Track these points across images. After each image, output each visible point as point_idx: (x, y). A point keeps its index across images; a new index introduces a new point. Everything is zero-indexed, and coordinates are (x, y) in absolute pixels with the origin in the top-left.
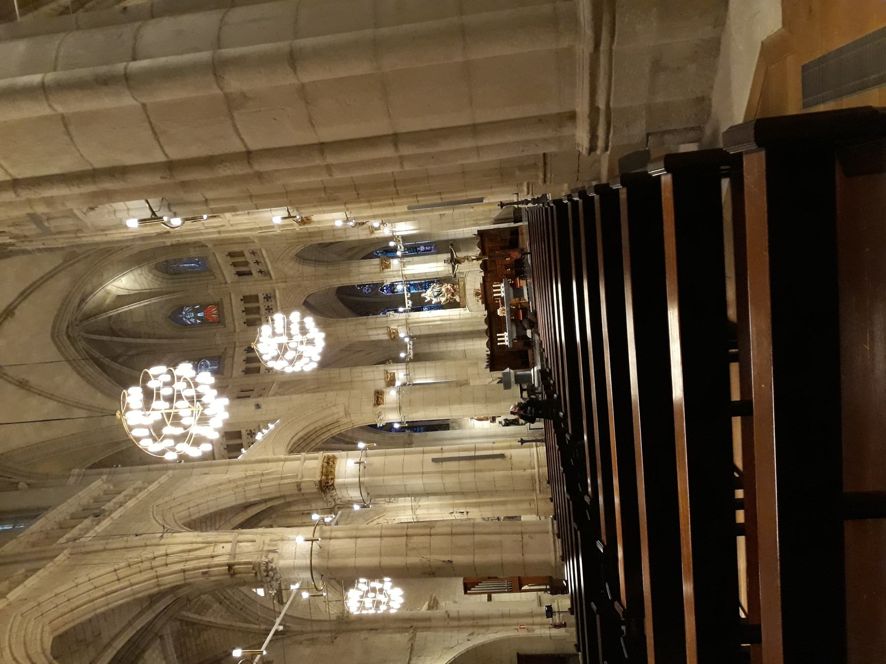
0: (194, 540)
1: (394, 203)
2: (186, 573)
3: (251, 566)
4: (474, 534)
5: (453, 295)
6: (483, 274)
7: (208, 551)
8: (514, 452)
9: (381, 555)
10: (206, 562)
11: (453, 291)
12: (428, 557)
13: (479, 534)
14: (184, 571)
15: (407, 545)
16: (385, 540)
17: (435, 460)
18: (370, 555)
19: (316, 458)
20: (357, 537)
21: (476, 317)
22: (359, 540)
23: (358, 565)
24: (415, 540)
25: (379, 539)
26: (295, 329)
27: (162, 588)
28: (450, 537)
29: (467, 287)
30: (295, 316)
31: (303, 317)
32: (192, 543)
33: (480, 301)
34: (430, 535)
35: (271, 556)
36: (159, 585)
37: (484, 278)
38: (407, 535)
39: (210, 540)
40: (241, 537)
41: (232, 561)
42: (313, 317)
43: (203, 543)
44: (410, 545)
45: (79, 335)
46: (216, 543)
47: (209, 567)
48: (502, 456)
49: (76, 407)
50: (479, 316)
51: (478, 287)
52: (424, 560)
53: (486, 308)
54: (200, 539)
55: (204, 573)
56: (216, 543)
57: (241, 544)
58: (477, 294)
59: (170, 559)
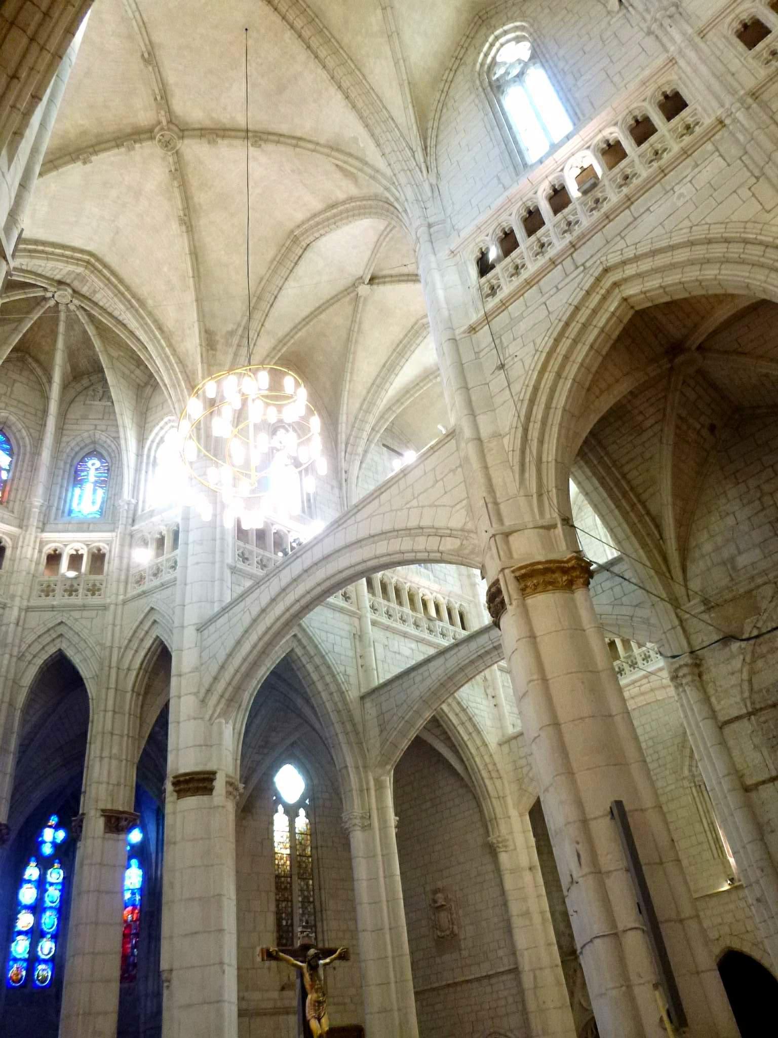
45: (53, 296)
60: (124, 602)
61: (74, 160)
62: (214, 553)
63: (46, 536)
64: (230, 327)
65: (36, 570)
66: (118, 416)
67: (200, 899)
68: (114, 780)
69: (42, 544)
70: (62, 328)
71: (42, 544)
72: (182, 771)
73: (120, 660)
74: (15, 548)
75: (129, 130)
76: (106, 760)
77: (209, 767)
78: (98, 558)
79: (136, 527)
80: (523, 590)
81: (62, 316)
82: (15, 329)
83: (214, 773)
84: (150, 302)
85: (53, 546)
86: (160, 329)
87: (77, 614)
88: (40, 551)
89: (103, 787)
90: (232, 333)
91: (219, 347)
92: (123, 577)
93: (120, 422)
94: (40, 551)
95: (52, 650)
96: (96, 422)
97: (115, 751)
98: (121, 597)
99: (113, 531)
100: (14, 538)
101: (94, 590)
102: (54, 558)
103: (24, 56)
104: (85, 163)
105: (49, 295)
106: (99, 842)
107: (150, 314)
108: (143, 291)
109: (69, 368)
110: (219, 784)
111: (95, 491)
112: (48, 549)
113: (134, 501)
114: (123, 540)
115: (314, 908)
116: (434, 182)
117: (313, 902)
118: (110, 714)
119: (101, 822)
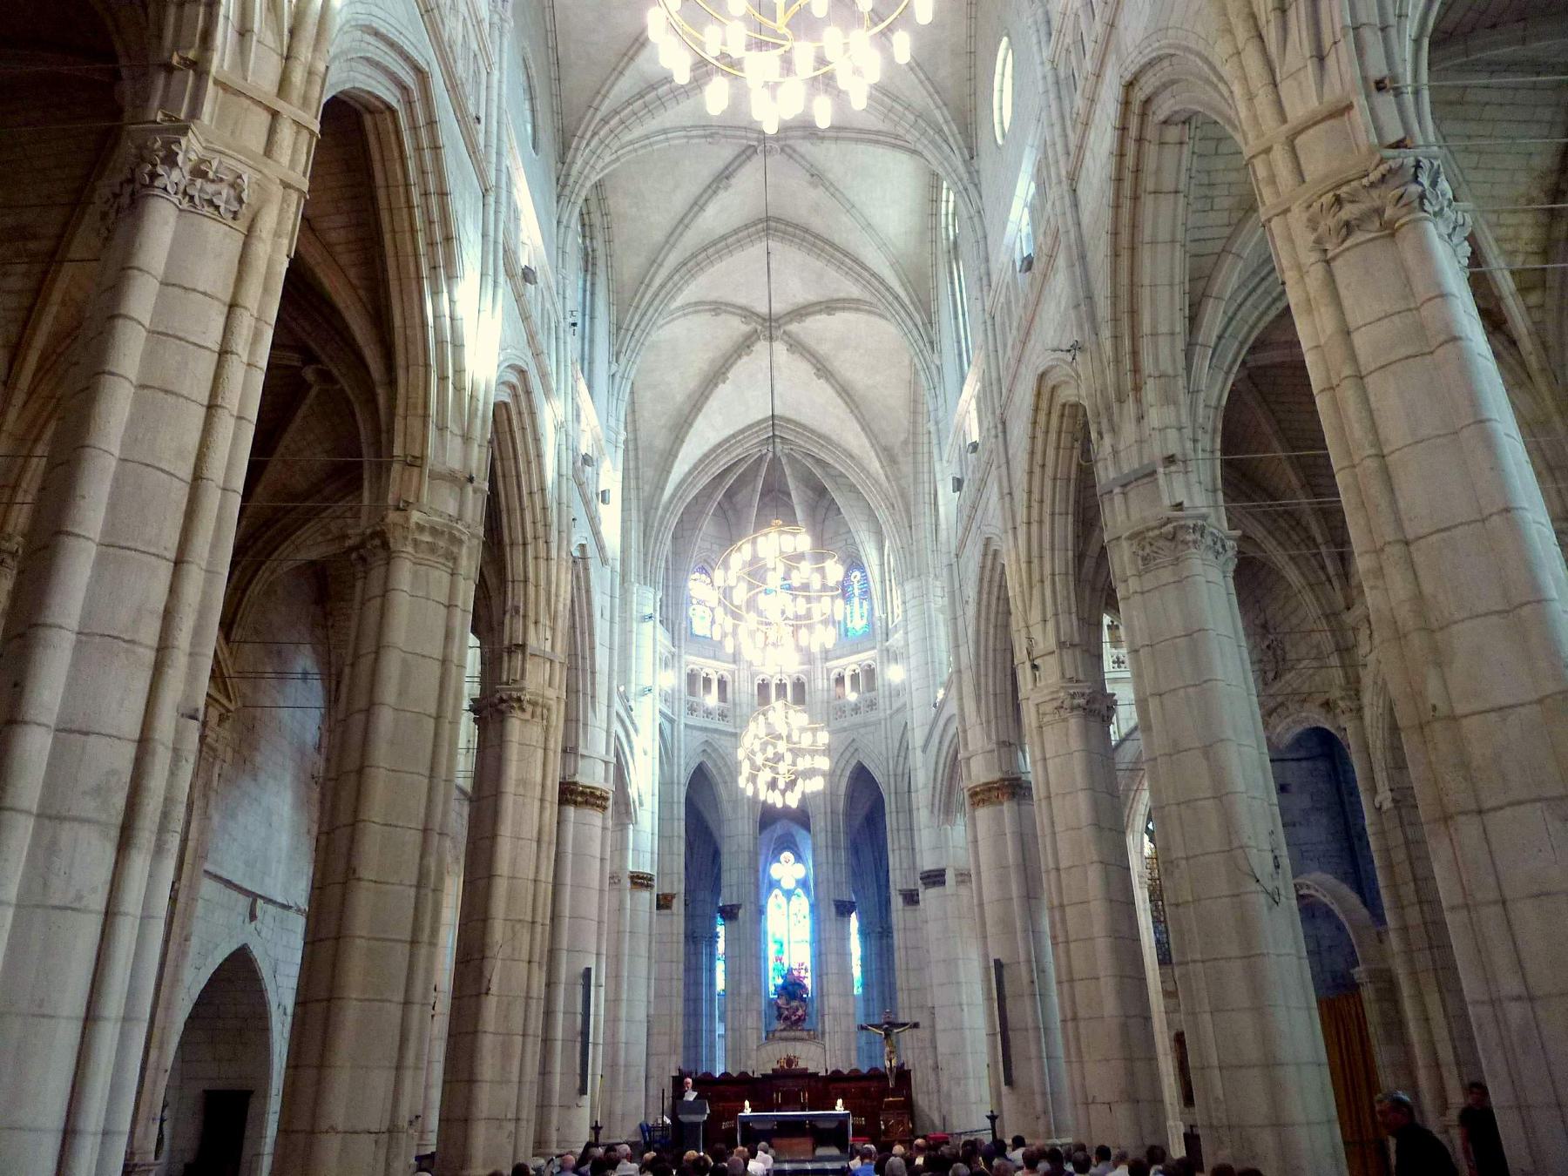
0: (561, 599)
1: (1057, 944)
2: (522, 585)
3: (518, 677)
4: (524, 1035)
5: (787, 1018)
6: (822, 1073)
7: (544, 619)
8: (586, 1112)
9: (513, 878)
10: (531, 614)
11: (793, 1018)
12: (500, 956)
13: (524, 1044)
14: (526, 581)
15: (520, 921)
16: (531, 886)
17: (588, 970)
18: (514, 862)
19: (606, 779)
20: (539, 841)
21: (748, 1057)
22: (534, 845)
23: (500, 839)
24: (526, 938)
25: (531, 876)
26: (804, 763)
27: (508, 549)
28: (523, 994)
29: (799, 1045)
30: (824, 763)
31: (824, 774)
32: (557, 596)
33: (776, 1066)
34: (530, 962)
35: (529, 708)
36: (512, 545)
37: (815, 1075)
38: (533, 923)
39: (560, 622)
40: (557, 666)
41: (528, 651)
42: (824, 793)
43: (556, 612)
44: (518, 926)
46: (553, 629)
47: (525, 617)
48: (583, 1091)
49: (677, 437)
50: (750, 1062)
51: (802, 1065)
52: (496, 949)
53: (765, 1076)
54: (561, 607)
55: (517, 612)
56: (553, 629)
57: (548, 665)
58: (789, 1061)
59: (542, 563)
60: (891, 716)
61: (716, 385)
62: (928, 676)
63: (830, 664)
64: (902, 437)
65: (829, 695)
66: (855, 535)
67: (944, 961)
68: (905, 866)
69: (829, 671)
70: (787, 471)
71: (829, 671)
72: (927, 868)
73: (895, 770)
74: (809, 682)
75: (741, 339)
76: (897, 852)
77: (941, 866)
78: (870, 673)
79: (890, 641)
80: (975, 805)
81: (784, 461)
82: (754, 490)
83: (944, 870)
84: (834, 437)
85: (836, 671)
86: (851, 456)
87: (862, 731)
88: (828, 679)
89: (898, 872)
90: (905, 442)
91: (901, 459)
92: (887, 693)
93: (858, 540)
94: (828, 679)
95: (854, 762)
96: (844, 537)
97: (903, 842)
98: (888, 712)
99: (874, 648)
100: (807, 673)
101: (872, 705)
102: (840, 680)
103: (537, 868)
104: (724, 382)
105: (764, 451)
106: (900, 913)
107: (838, 446)
108: (824, 429)
109: (810, 493)
110: (950, 877)
111: (861, 604)
112: (833, 676)
113: (884, 616)
114: (881, 658)
115: (1166, 927)
116: (938, 363)
117: (1165, 921)
118: (894, 814)
119: (900, 899)
